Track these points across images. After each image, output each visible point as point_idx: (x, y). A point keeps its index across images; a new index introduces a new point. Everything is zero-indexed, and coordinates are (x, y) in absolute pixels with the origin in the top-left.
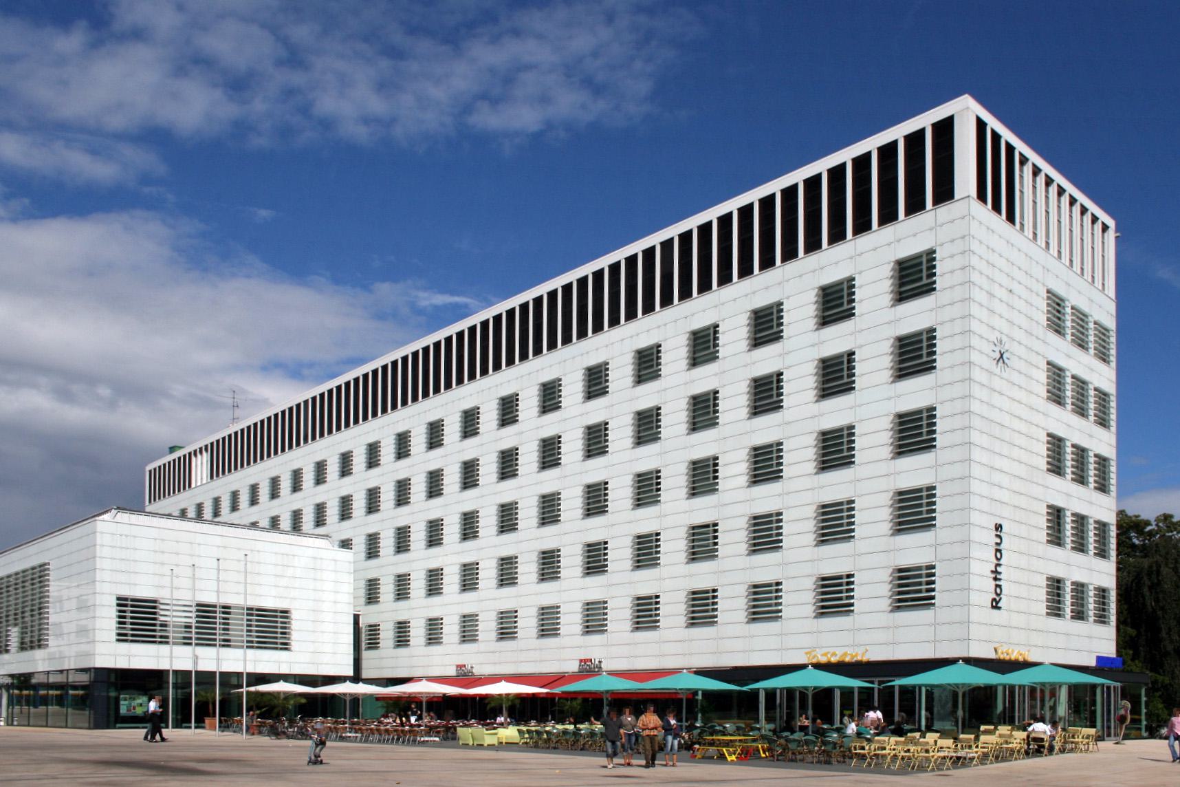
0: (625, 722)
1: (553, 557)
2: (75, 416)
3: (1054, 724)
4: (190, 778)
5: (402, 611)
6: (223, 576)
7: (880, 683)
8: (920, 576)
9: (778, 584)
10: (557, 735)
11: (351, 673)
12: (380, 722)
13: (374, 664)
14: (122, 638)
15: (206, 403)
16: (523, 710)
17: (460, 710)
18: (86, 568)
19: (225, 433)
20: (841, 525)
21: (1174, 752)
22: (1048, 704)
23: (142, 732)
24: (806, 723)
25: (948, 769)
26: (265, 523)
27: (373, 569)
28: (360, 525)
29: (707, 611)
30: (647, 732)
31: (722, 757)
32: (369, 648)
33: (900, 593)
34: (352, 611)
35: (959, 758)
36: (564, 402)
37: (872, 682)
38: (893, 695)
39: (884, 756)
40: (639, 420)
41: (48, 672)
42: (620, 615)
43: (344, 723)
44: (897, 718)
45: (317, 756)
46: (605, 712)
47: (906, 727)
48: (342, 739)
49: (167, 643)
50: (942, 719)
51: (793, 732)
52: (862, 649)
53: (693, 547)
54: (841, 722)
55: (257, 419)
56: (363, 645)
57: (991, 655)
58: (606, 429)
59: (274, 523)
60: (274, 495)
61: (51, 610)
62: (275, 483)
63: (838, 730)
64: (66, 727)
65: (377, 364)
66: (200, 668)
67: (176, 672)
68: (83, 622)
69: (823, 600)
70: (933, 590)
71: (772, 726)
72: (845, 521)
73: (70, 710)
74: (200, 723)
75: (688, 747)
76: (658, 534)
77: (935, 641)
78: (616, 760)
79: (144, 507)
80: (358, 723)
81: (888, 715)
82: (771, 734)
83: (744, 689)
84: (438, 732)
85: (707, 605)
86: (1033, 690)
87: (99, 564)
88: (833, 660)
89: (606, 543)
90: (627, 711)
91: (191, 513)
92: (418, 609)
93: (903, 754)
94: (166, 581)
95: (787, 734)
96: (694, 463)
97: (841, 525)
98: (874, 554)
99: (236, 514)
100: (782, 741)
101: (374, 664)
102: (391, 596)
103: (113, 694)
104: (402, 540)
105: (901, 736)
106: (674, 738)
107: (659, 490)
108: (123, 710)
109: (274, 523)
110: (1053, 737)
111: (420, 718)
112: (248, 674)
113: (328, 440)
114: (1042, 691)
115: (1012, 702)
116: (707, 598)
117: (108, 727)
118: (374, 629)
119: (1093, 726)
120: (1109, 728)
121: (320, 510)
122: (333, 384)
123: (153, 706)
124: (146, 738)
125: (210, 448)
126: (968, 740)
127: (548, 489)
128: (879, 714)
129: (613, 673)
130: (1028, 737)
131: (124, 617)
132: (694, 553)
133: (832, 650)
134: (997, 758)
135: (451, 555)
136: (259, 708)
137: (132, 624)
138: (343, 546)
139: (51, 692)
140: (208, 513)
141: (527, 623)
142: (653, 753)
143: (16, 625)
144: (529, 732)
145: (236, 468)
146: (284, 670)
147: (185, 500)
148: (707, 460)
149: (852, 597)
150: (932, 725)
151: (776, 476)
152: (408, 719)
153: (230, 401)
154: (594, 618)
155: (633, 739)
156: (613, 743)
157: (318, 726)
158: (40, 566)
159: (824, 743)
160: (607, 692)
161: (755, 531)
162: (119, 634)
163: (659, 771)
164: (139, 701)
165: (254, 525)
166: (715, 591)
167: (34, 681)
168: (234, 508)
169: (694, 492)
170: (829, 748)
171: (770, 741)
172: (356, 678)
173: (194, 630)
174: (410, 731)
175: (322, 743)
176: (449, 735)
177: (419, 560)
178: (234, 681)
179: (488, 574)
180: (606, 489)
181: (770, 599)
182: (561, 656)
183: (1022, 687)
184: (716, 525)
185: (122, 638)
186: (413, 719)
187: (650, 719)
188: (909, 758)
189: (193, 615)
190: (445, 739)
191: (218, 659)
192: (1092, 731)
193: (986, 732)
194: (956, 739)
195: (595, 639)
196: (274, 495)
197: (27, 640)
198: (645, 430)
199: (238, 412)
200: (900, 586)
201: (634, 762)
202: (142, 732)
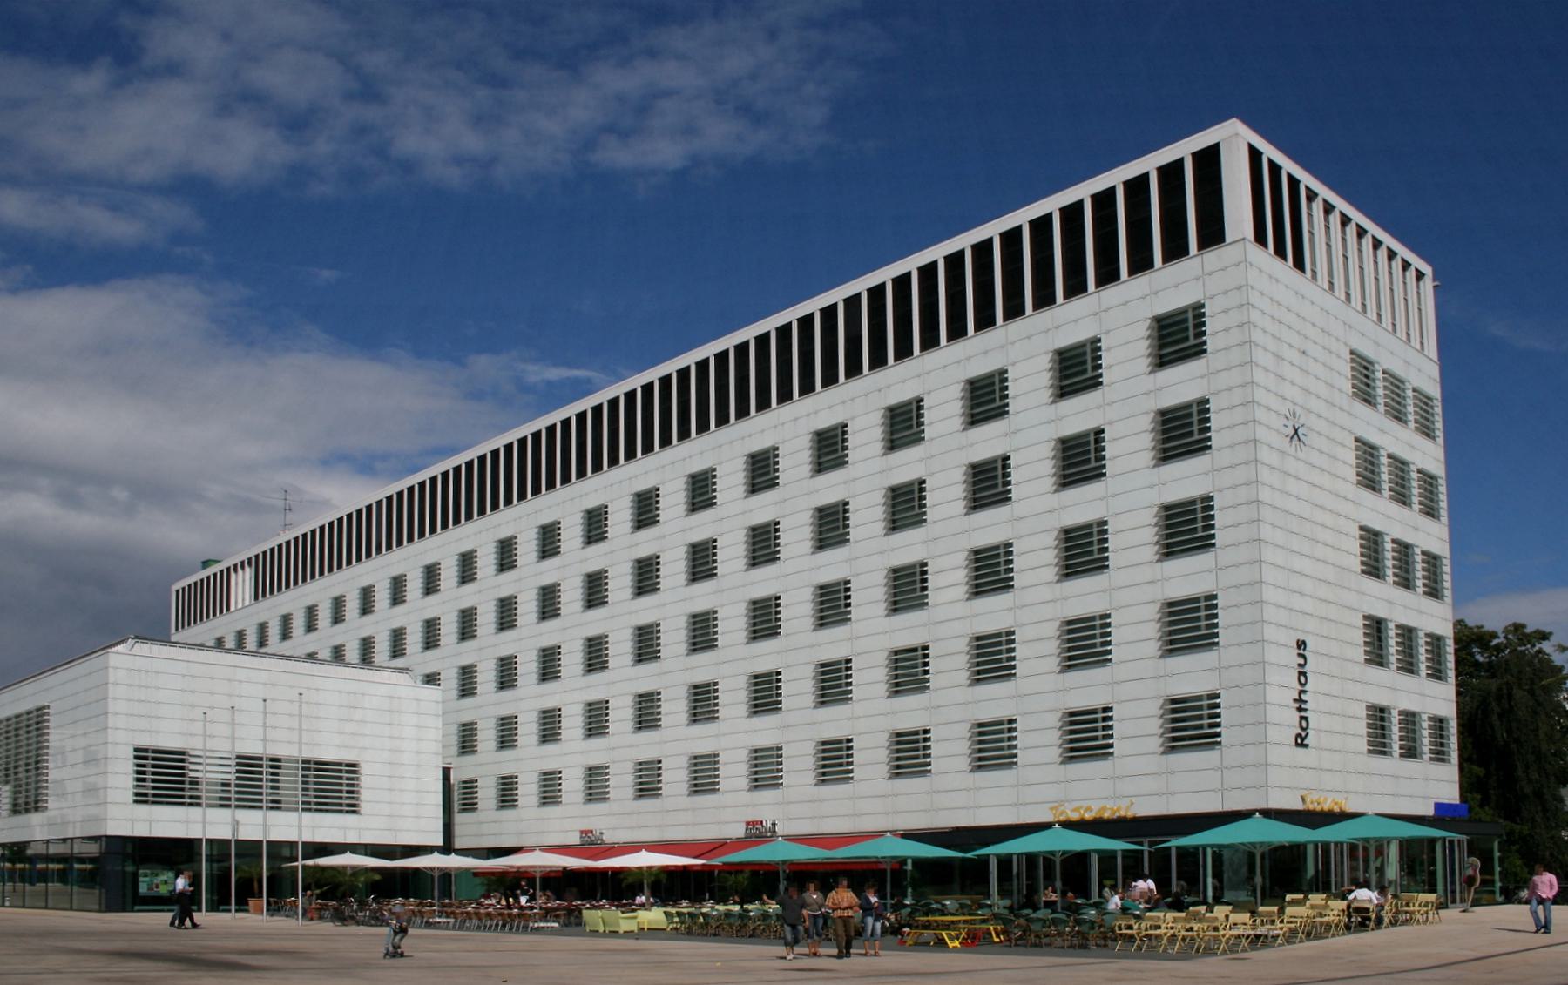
0: (809, 901)
1: (708, 692)
2: (85, 524)
3: (1382, 890)
4: (229, 973)
5: (507, 762)
6: (270, 720)
7: (1151, 844)
8: (1200, 708)
9: (1011, 721)
10: (718, 918)
11: (440, 842)
12: (480, 904)
13: (469, 830)
14: (141, 798)
15: (248, 506)
16: (669, 886)
17: (585, 888)
18: (96, 711)
19: (274, 543)
20: (1094, 645)
21: (1537, 919)
22: (1373, 866)
23: (167, 916)
24: (1054, 897)
25: (1244, 951)
26: (325, 654)
27: (469, 710)
28: (450, 655)
29: (917, 757)
30: (839, 913)
31: (941, 943)
32: (464, 811)
33: (1174, 730)
34: (440, 763)
35: (1258, 937)
36: (720, 498)
37: (1141, 844)
38: (1171, 860)
39: (1158, 937)
40: (821, 518)
41: (47, 841)
42: (799, 765)
43: (432, 905)
44: (1174, 889)
45: (396, 947)
46: (782, 887)
47: (1188, 899)
48: (429, 925)
49: (199, 805)
50: (1235, 887)
51: (1036, 909)
52: (1126, 802)
53: (896, 677)
54: (1101, 895)
55: (316, 525)
56: (456, 807)
57: (1297, 805)
58: (777, 530)
59: (338, 654)
60: (337, 618)
61: (50, 765)
62: (338, 603)
63: (1096, 905)
64: (71, 909)
65: (473, 454)
66: (241, 837)
67: (210, 841)
68: (92, 779)
69: (1072, 741)
70: (1218, 725)
71: (1007, 902)
72: (1099, 640)
73: (75, 888)
74: (242, 905)
75: (895, 930)
76: (849, 661)
77: (1222, 790)
78: (797, 949)
79: (169, 635)
80: (450, 905)
81: (1163, 884)
82: (1006, 912)
83: (969, 855)
84: (557, 916)
85: (917, 749)
86: (1353, 848)
87: (112, 706)
88: (1088, 816)
89: (779, 673)
90: (812, 886)
91: (230, 643)
92: (528, 760)
93: (1183, 933)
94: (198, 727)
95: (1028, 911)
96: (895, 571)
97: (1094, 645)
98: (1138, 681)
99: (287, 643)
100: (1022, 921)
101: (469, 830)
102: (493, 744)
103: (130, 868)
104: (506, 674)
105: (1180, 910)
106: (876, 920)
107: (849, 605)
108: (143, 889)
109: (338, 654)
110: (1381, 907)
111: (532, 898)
112: (304, 844)
113: (408, 550)
114: (1365, 849)
115: (1326, 863)
116: (917, 741)
117: (124, 910)
118: (470, 786)
119: (1434, 891)
120: (1453, 892)
121: (398, 637)
122: (414, 480)
123: (181, 883)
124: (172, 924)
125: (255, 561)
126: (1270, 914)
127: (700, 606)
128: (1151, 884)
129: (790, 839)
130: (1349, 907)
131: (144, 773)
132: (897, 685)
133: (1085, 804)
134: (1308, 935)
135: (573, 691)
136: (318, 886)
137: (154, 781)
138: (428, 682)
139: (51, 866)
140: (251, 642)
141: (675, 777)
142: (848, 939)
143: (7, 782)
144: (679, 914)
145: (272, 592)
146: (352, 838)
147: (222, 626)
148: (913, 566)
149: (1111, 736)
150: (1222, 896)
151: (1005, 585)
152: (517, 900)
153: (281, 504)
154: (765, 769)
155: (821, 922)
156: (794, 927)
157: (397, 909)
158: (38, 710)
159: (1078, 922)
160: (784, 862)
161: (978, 656)
162: (137, 794)
163: (856, 962)
164: (164, 878)
165: (311, 657)
166: (926, 731)
167: (29, 852)
168: (286, 635)
169: (896, 607)
170: (1085, 928)
171: (1005, 921)
172: (447, 848)
173: (233, 789)
174: (519, 915)
175: (403, 931)
176: (572, 920)
177: (528, 699)
178: (286, 852)
179: (621, 715)
180: (778, 605)
181: (1001, 740)
182: (723, 816)
183: (1338, 844)
184: (926, 648)
185: (141, 798)
186: (523, 900)
187: (843, 897)
188: (1192, 939)
189: (233, 769)
190: (567, 925)
191: (265, 825)
192: (1432, 897)
193: (1293, 903)
194: (1253, 913)
195: (767, 795)
196: (337, 618)
197: (21, 801)
198: (828, 531)
199: (290, 517)
200: (1174, 720)
201: (822, 951)
202: (167, 916)
